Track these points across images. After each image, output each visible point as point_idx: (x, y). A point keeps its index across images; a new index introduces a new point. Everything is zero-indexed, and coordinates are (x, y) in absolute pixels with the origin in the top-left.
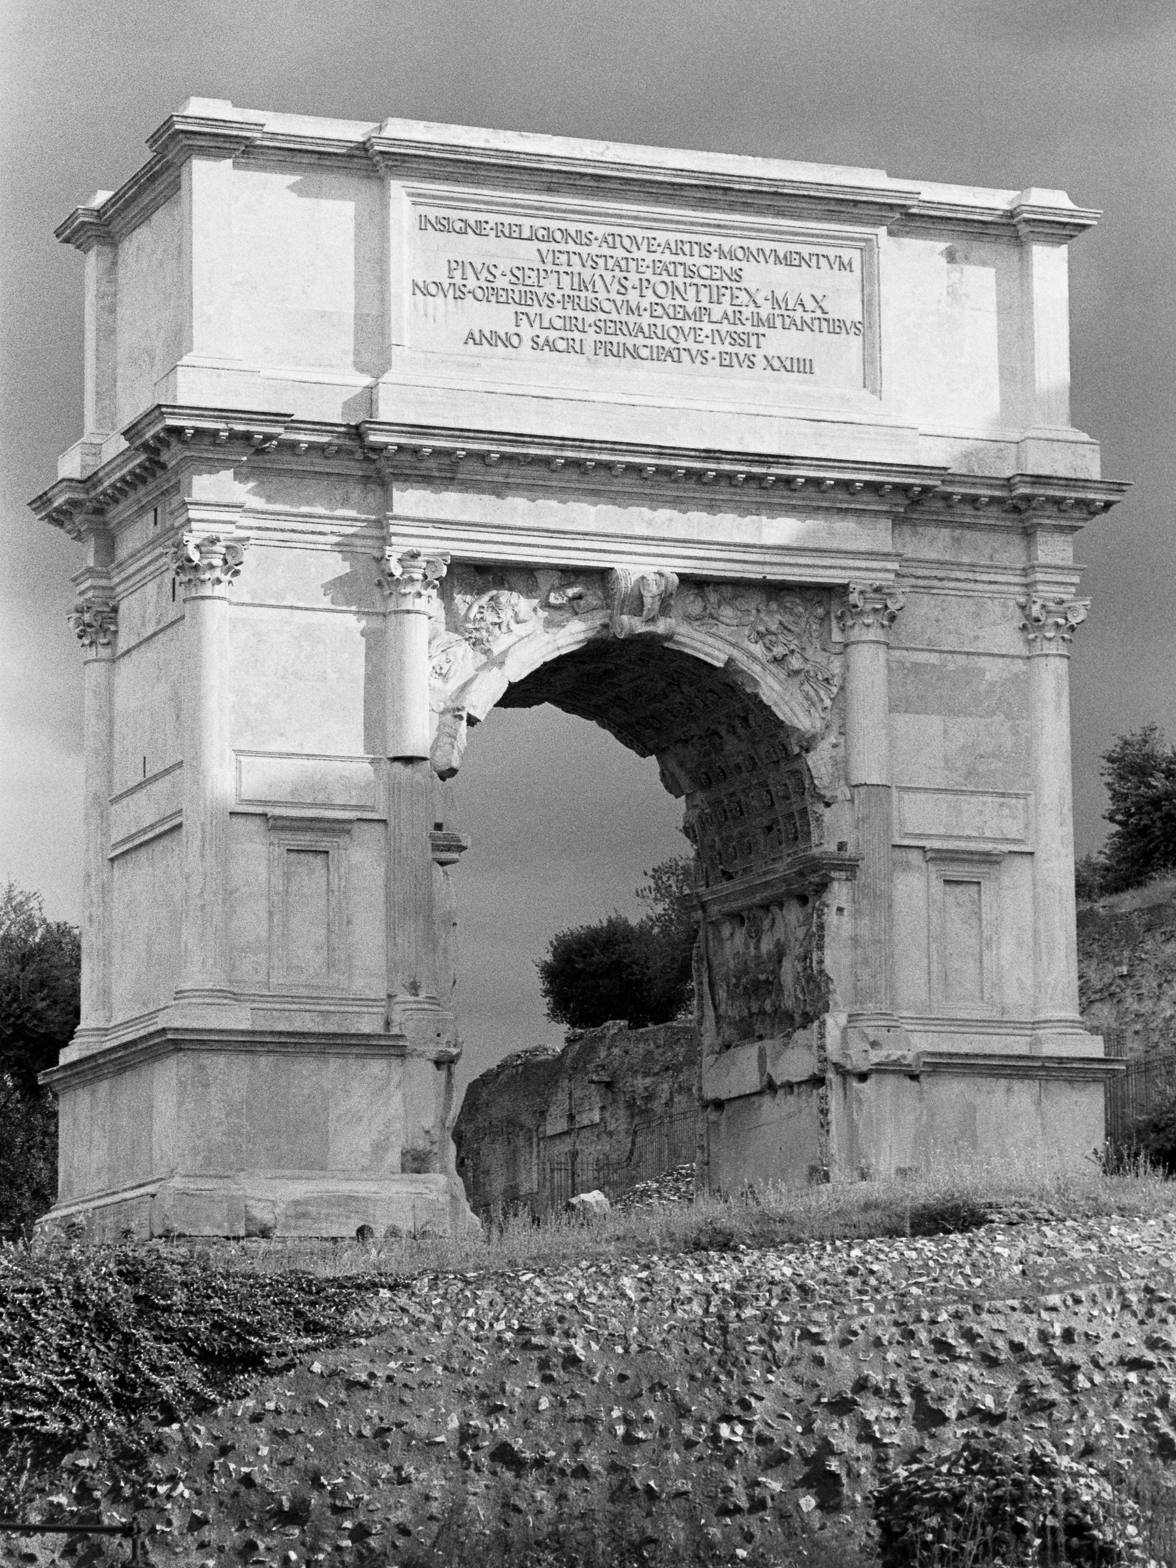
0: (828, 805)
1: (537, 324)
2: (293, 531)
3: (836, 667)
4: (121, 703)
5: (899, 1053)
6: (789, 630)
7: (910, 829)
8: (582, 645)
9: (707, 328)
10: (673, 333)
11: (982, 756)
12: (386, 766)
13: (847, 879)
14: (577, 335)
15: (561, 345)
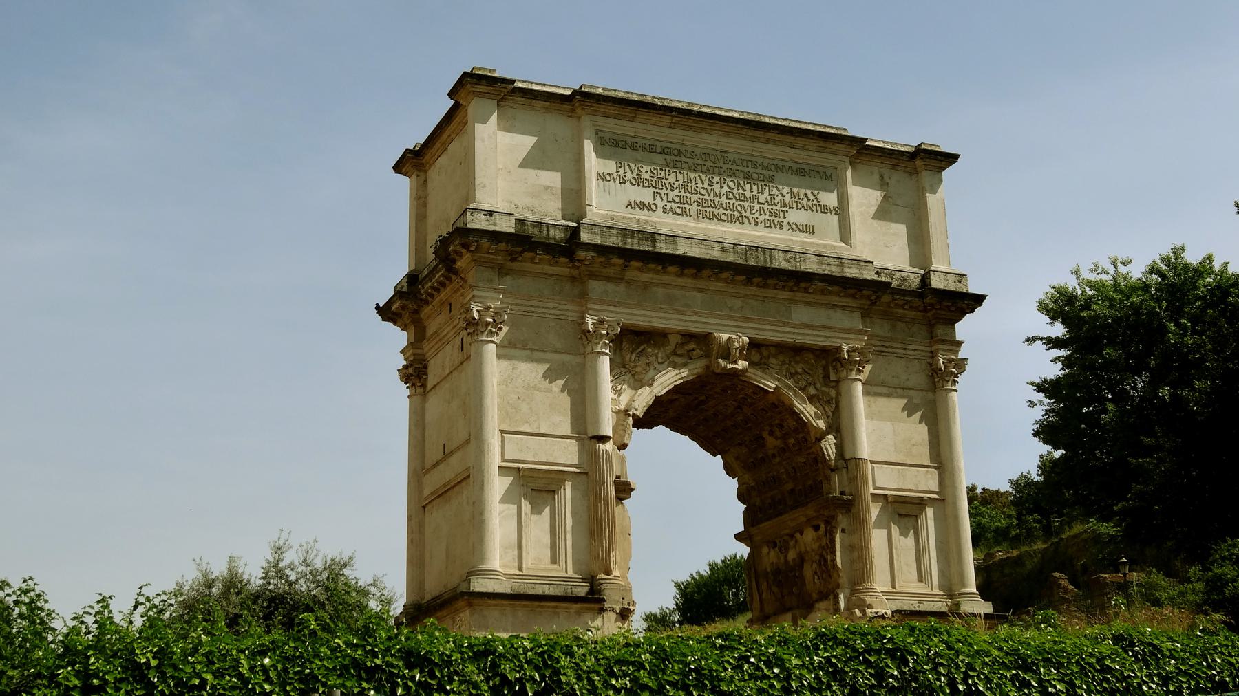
0: (833, 470)
1: (665, 199)
2: (532, 306)
3: (833, 393)
4: (428, 418)
5: (883, 611)
6: (807, 373)
7: (877, 485)
8: (695, 376)
9: (757, 207)
10: (739, 208)
11: (914, 445)
12: (587, 442)
13: (846, 512)
14: (686, 206)
15: (679, 211)
